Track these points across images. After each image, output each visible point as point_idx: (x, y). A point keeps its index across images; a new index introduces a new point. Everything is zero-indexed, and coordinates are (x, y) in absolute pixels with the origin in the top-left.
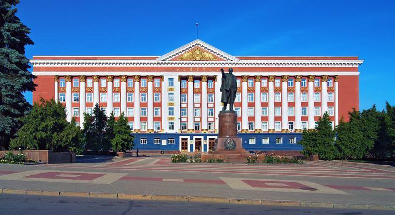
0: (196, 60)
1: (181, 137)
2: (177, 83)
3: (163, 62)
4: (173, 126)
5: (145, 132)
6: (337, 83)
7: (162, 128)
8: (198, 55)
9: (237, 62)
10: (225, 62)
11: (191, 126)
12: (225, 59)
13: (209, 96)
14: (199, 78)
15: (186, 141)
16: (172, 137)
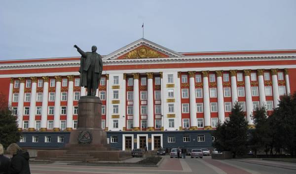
0: (141, 58)
1: (124, 136)
2: (122, 83)
3: (109, 61)
4: (117, 124)
6: (287, 76)
10: (170, 59)
11: (137, 124)
13: (101, 93)
14: (145, 76)
15: (130, 139)
16: (117, 136)
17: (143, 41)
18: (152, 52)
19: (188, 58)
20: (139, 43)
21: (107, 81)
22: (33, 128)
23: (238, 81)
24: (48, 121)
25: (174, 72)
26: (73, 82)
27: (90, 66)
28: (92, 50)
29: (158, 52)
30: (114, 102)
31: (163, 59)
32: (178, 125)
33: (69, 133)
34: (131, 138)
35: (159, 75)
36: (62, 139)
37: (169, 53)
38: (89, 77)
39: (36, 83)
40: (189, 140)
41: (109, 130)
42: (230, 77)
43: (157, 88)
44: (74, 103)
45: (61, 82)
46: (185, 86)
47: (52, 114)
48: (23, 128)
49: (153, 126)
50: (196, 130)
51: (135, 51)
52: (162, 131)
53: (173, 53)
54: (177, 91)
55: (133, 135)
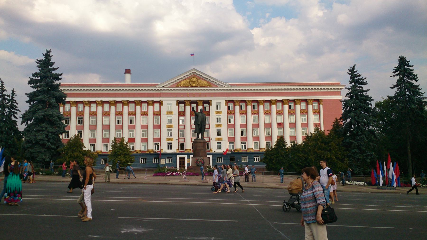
0: (192, 87)
1: (178, 157)
3: (163, 88)
5: (146, 152)
7: (161, 148)
8: (194, 82)
9: (230, 88)
10: (218, 88)
12: (219, 86)
15: (183, 160)
17: (194, 71)
18: (202, 82)
19: (234, 88)
20: (191, 73)
24: (141, 143)
25: (222, 100)
26: (152, 107)
29: (208, 82)
30: (169, 126)
31: (212, 88)
32: (225, 147)
34: (184, 158)
36: (105, 161)
37: (218, 83)
39: (189, 107)
40: (221, 161)
42: (246, 105)
46: (231, 113)
47: (145, 136)
49: (190, 148)
50: (240, 151)
51: (187, 80)
52: (211, 152)
53: (218, 82)
54: (224, 117)
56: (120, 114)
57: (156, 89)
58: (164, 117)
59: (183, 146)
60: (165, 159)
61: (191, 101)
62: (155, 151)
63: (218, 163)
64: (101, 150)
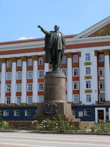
1: (96, 109)
3: (80, 39)
7: (80, 101)
15: (102, 113)
21: (80, 58)
22: (15, 104)
23: (18, 66)
27: (54, 44)
28: (55, 29)
33: (36, 108)
34: (103, 111)
35: (79, 54)
38: (53, 54)
41: (82, 103)
43: (76, 65)
44: (39, 80)
45: (17, 63)
48: (6, 103)
51: (105, 28)
55: (105, 108)
56: (19, 69)
57: (74, 40)
58: (82, 69)
59: (10, 100)
60: (82, 112)
61: (6, 58)
62: (74, 104)
63: (89, 116)
64: (26, 103)
